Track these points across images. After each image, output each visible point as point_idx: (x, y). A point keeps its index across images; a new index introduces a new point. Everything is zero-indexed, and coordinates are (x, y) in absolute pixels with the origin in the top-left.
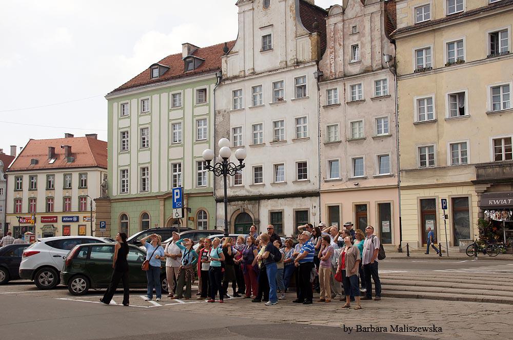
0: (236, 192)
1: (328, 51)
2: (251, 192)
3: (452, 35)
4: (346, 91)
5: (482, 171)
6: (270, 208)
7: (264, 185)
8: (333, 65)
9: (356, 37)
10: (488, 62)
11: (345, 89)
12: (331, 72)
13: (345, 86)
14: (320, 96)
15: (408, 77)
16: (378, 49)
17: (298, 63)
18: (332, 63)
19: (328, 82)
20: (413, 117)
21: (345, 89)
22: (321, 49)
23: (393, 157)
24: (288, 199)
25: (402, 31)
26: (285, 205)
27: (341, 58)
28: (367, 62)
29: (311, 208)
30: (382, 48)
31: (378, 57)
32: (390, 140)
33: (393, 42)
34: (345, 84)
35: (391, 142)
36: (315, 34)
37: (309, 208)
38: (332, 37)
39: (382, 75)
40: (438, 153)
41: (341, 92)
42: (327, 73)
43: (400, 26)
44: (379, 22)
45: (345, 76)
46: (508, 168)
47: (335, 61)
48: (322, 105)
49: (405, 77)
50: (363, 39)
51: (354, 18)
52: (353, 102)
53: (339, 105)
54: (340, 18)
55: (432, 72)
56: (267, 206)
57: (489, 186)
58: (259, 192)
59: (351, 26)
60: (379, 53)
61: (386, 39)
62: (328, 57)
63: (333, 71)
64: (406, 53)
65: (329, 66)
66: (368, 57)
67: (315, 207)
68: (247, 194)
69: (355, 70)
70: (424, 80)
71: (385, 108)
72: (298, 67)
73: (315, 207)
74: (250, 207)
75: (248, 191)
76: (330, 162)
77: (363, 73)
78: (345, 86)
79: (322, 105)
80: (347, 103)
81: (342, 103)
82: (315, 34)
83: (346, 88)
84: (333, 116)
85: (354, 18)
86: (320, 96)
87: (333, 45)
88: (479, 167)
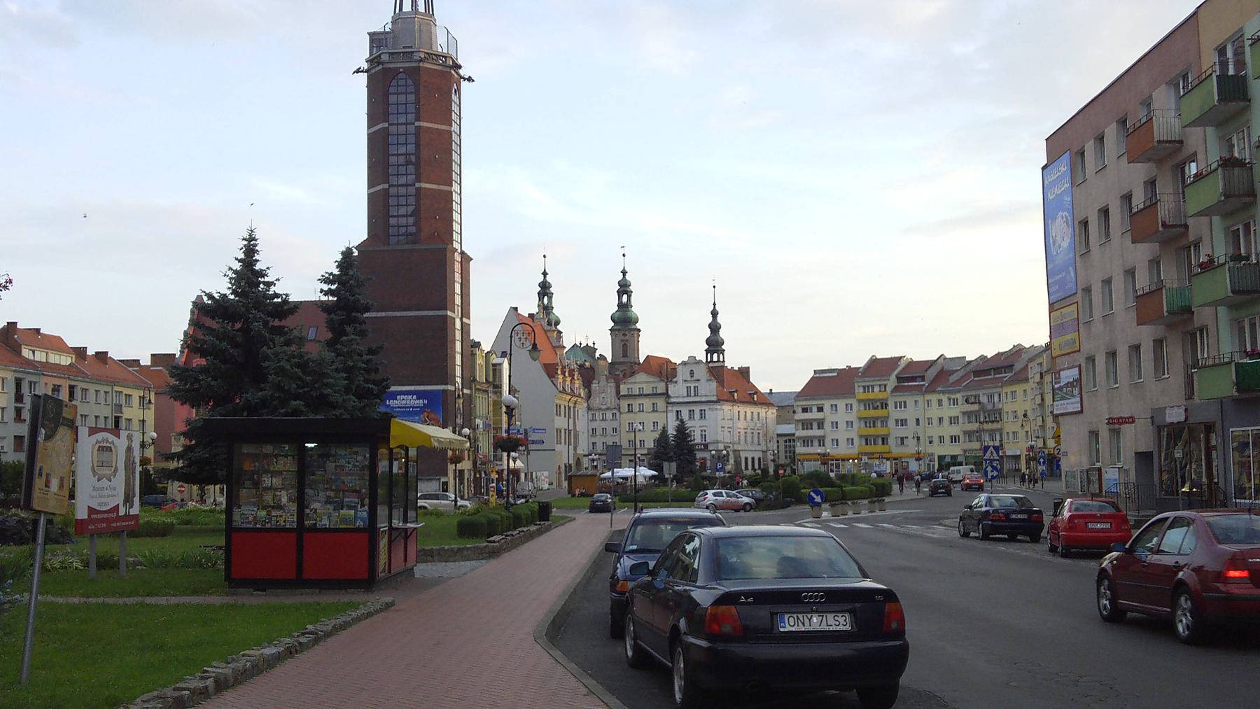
1: (592, 398)
3: (641, 401)
16: (613, 401)
22: (589, 396)
25: (622, 396)
28: (609, 405)
31: (613, 404)
33: (619, 399)
35: (618, 437)
36: (586, 390)
41: (599, 415)
42: (591, 406)
43: (621, 394)
44: (614, 391)
45: (600, 409)
47: (596, 402)
54: (597, 385)
61: (617, 399)
62: (591, 400)
64: (624, 404)
70: (631, 415)
71: (615, 424)
76: (593, 443)
82: (586, 390)
84: (594, 425)
88: (648, 449)
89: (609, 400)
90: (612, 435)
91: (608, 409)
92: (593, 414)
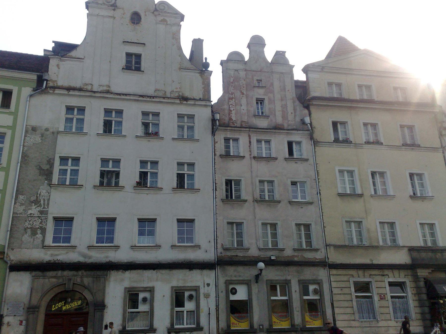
0: (56, 255)
2: (90, 257)
4: (252, 144)
5: (415, 254)
6: (127, 284)
7: (117, 247)
8: (233, 112)
9: (261, 91)
10: (403, 149)
11: (250, 142)
12: (230, 119)
13: (250, 138)
14: (215, 143)
15: (326, 145)
17: (184, 99)
18: (232, 109)
19: (228, 128)
20: (336, 187)
21: (250, 142)
23: (315, 230)
24: (164, 271)
26: (157, 280)
27: (244, 107)
29: (201, 287)
30: (295, 110)
32: (312, 208)
33: (307, 107)
34: (249, 136)
37: (199, 287)
38: (232, 83)
39: (295, 137)
40: (368, 230)
46: (439, 254)
48: (218, 154)
49: (324, 145)
50: (271, 95)
51: (258, 71)
52: (258, 158)
53: (244, 157)
55: (352, 146)
56: (122, 280)
57: (430, 271)
58: (107, 257)
59: (255, 78)
60: (292, 113)
63: (234, 119)
65: (227, 112)
66: (279, 114)
67: (208, 285)
68: (82, 259)
69: (263, 123)
72: (185, 102)
73: (208, 285)
74: (87, 281)
75: (84, 256)
77: (270, 129)
78: (250, 138)
79: (218, 154)
80: (253, 157)
81: (247, 155)
83: (252, 140)
85: (258, 71)
86: (215, 143)
87: (232, 91)
88: (411, 249)
89: (278, 108)
90: (290, 203)
91: (277, 128)
92: (227, 140)
